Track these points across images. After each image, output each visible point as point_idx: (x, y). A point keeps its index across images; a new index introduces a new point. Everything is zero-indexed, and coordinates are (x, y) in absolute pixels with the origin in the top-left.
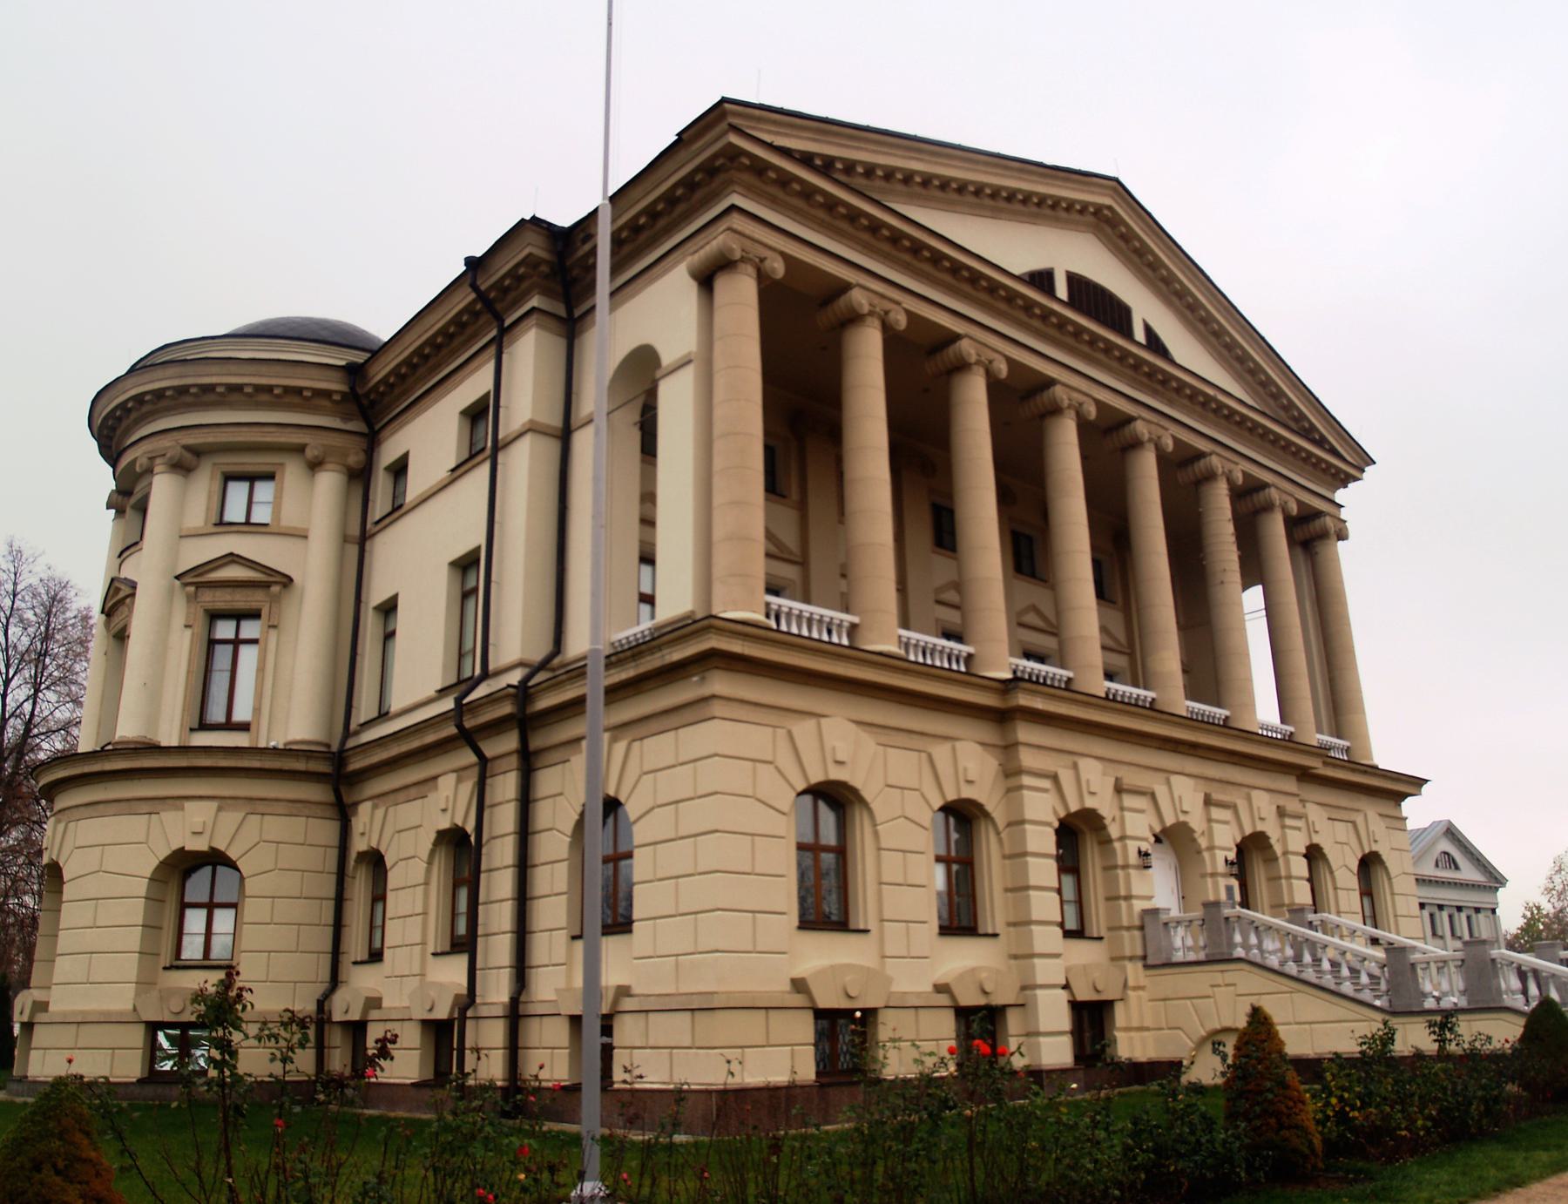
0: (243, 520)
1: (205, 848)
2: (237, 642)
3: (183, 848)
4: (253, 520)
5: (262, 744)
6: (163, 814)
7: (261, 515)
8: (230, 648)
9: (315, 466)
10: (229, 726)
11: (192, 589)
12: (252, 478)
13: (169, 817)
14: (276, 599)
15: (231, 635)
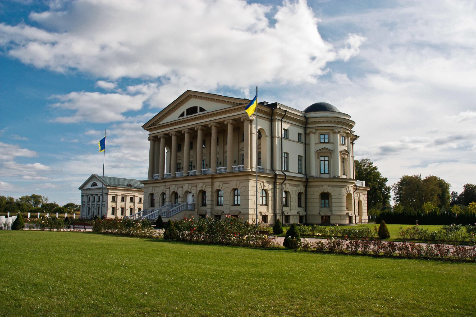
0: (323, 141)
1: (326, 192)
2: (324, 161)
3: (323, 192)
4: (325, 142)
5: (332, 177)
6: (320, 187)
7: (327, 141)
8: (323, 162)
9: (335, 133)
10: (325, 173)
11: (318, 153)
12: (324, 135)
13: (321, 188)
14: (331, 154)
15: (324, 160)
